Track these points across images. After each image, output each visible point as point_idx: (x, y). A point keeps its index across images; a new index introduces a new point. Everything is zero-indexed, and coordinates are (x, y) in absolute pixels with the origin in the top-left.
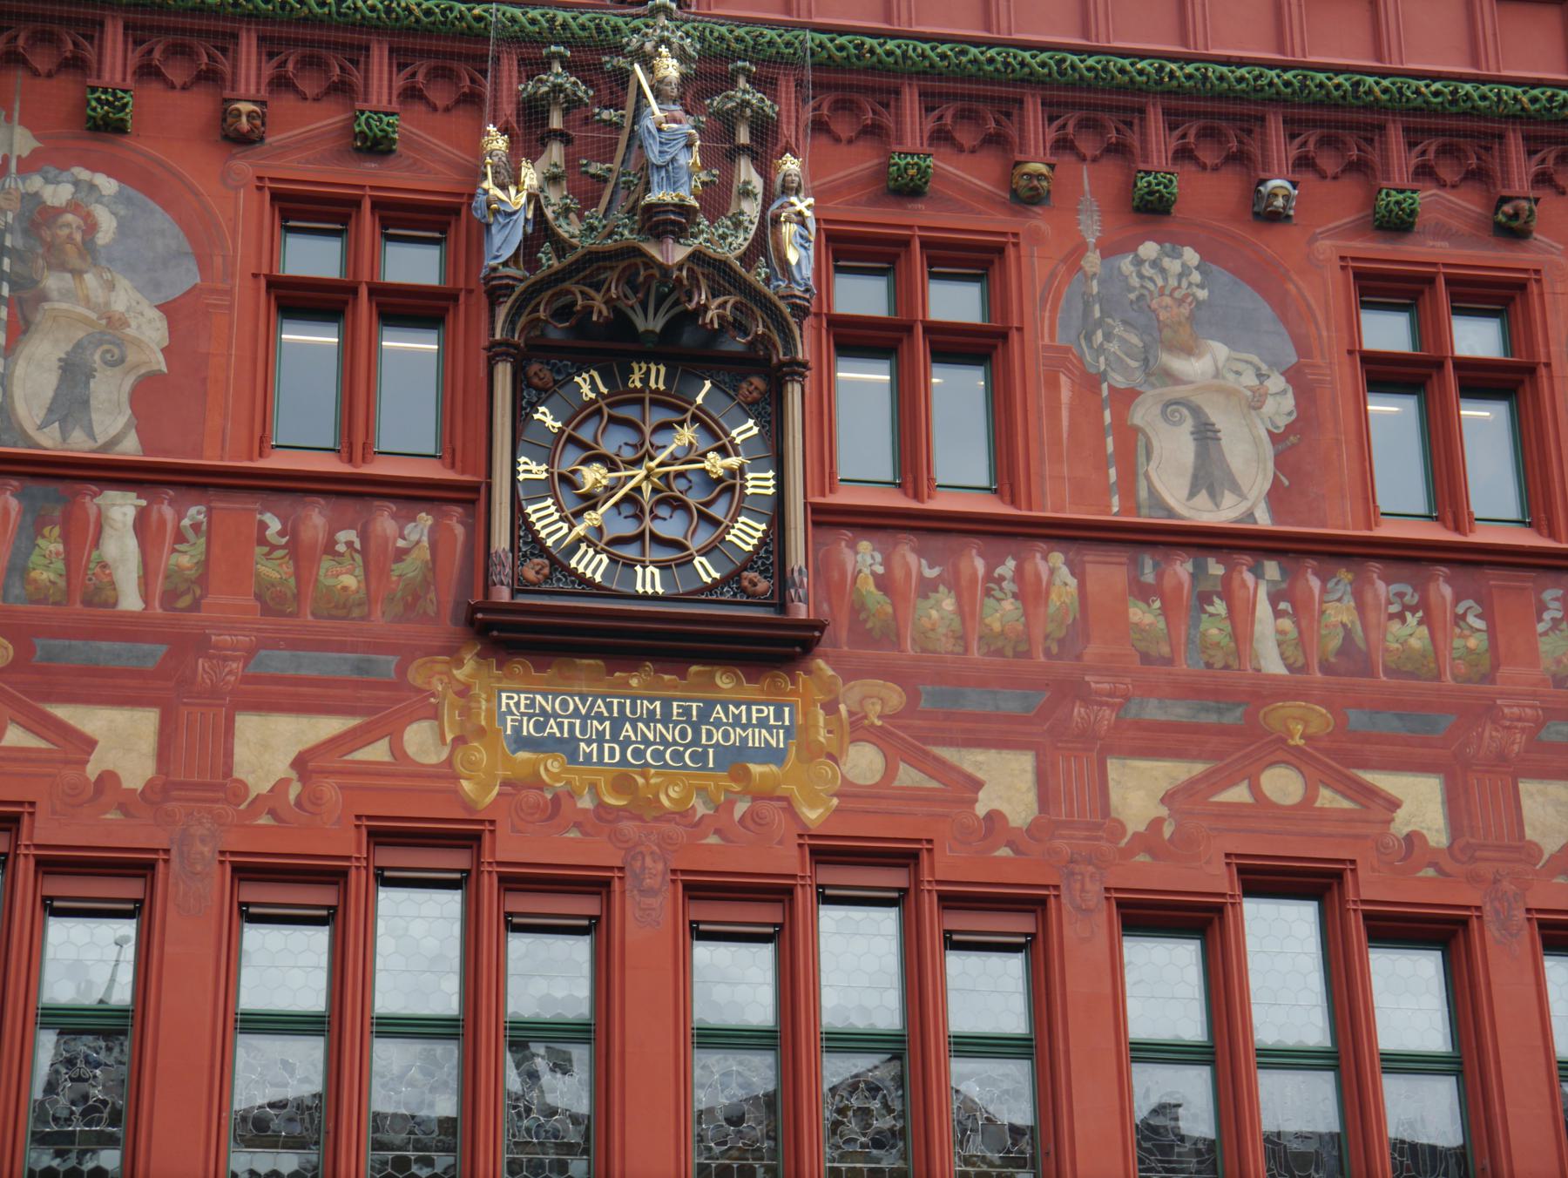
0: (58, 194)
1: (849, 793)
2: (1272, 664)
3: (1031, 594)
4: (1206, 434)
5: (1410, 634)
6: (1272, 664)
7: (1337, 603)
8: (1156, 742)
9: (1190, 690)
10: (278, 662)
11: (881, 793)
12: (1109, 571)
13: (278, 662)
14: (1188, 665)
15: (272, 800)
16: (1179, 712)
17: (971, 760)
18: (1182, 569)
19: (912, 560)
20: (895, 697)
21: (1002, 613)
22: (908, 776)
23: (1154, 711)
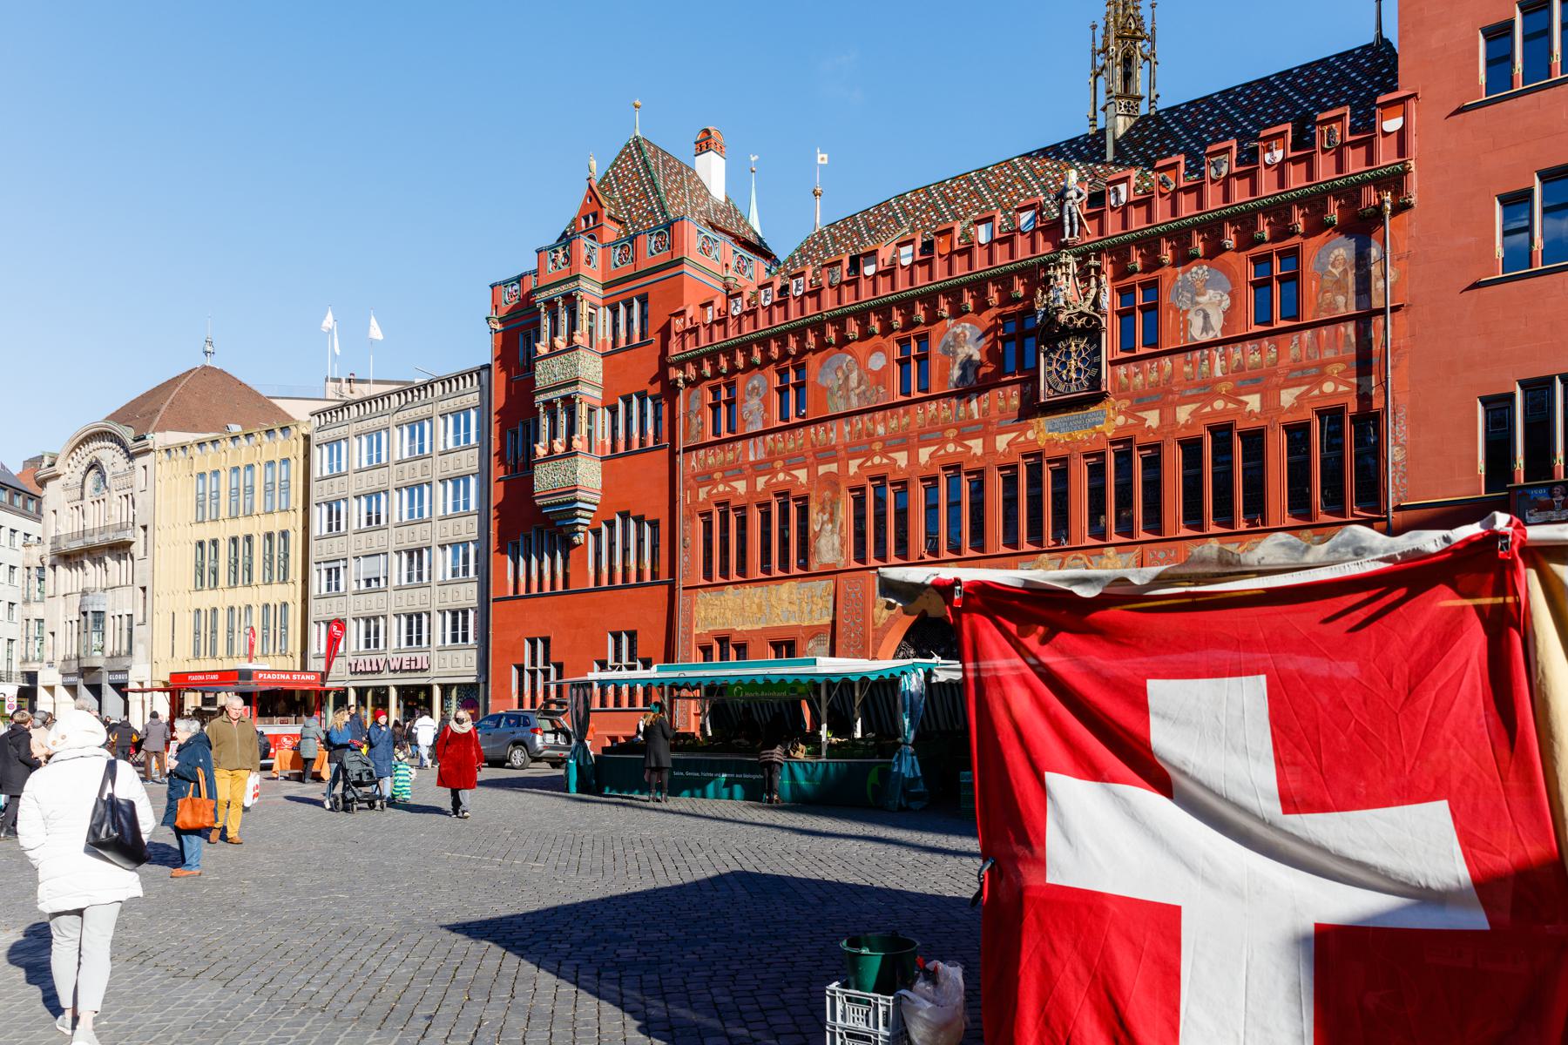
0: (959, 330)
1: (1117, 428)
2: (1218, 373)
3: (1160, 369)
4: (1206, 317)
5: (1257, 357)
6: (1218, 373)
7: (1236, 353)
8: (1186, 401)
9: (1198, 385)
10: (1003, 423)
11: (1125, 426)
12: (1179, 359)
13: (1003, 423)
14: (1198, 379)
15: (1003, 454)
16: (1195, 392)
17: (1143, 414)
18: (1198, 354)
19: (1133, 368)
20: (1128, 403)
21: (1154, 376)
22: (1131, 421)
23: (1188, 393)
